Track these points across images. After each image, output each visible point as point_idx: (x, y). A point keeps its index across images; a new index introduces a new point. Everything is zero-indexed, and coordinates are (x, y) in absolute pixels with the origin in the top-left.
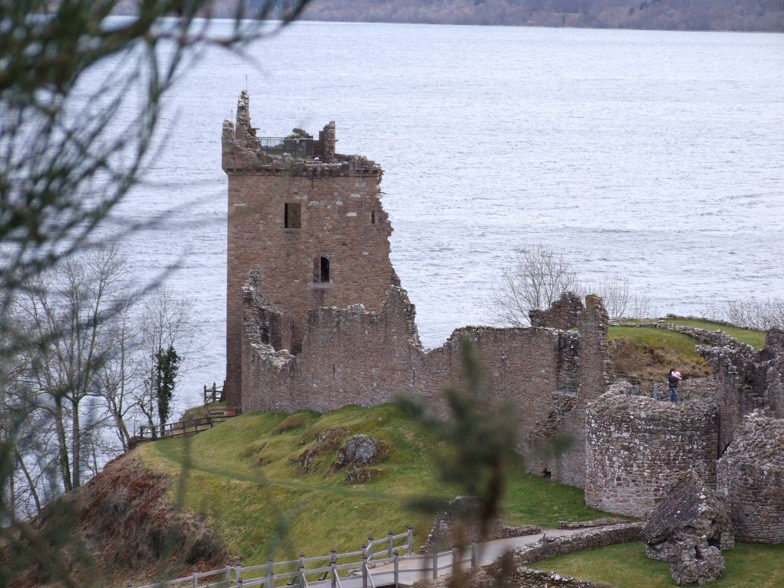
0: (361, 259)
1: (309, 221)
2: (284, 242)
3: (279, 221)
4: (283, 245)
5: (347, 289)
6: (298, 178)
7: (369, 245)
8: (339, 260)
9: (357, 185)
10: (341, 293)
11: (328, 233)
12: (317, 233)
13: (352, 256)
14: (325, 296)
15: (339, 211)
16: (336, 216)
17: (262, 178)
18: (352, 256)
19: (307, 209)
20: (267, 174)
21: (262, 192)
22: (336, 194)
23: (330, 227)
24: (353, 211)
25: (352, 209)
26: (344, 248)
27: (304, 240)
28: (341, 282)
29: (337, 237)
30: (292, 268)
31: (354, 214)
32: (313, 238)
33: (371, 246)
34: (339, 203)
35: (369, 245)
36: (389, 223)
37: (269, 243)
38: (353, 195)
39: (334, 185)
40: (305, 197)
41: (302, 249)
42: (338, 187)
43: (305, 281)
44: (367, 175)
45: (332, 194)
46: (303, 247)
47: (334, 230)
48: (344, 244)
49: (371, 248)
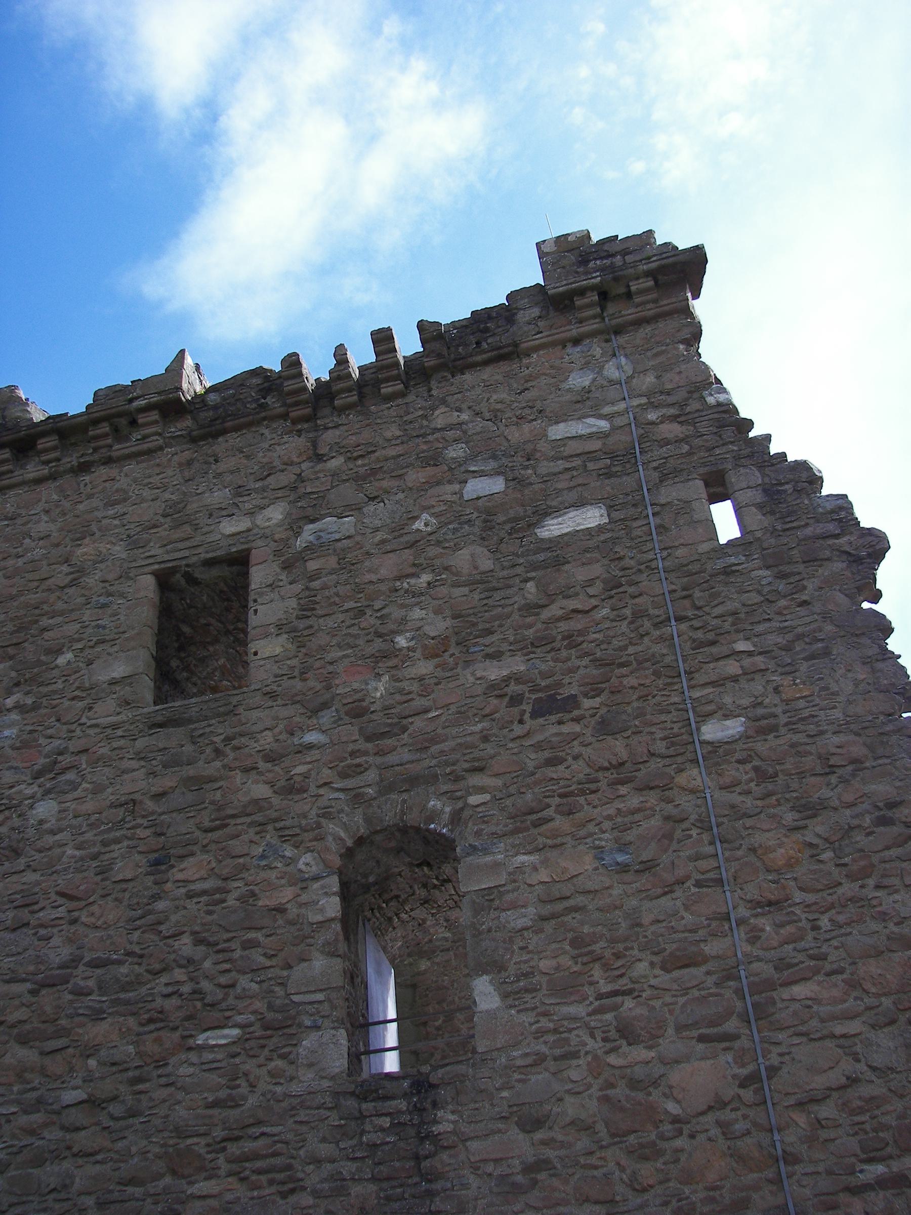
0: (694, 776)
1: (294, 629)
2: (137, 782)
3: (119, 670)
4: (131, 804)
5: (627, 1033)
6: (233, 440)
7: (732, 667)
8: (527, 822)
9: (579, 380)
10: (576, 1072)
11: (424, 668)
12: (348, 684)
13: (622, 773)
14: (446, 1121)
15: (488, 526)
16: (472, 557)
17: (49, 493)
18: (622, 773)
19: (287, 566)
20: (72, 459)
21: (38, 553)
22: (455, 452)
23: (438, 626)
24: (580, 504)
25: (572, 496)
26: (549, 729)
27: (267, 740)
28: (566, 988)
29: (494, 672)
30: (185, 946)
31: (592, 517)
32: (326, 718)
33: (749, 674)
34: (485, 486)
35: (732, 667)
36: (842, 504)
37: (46, 809)
38: (558, 431)
39: (441, 417)
40: (275, 514)
41: (258, 804)
42: (465, 417)
43: (280, 1028)
44: (629, 312)
45: (433, 459)
46: (261, 790)
47: (467, 637)
48: (552, 704)
49: (757, 687)
